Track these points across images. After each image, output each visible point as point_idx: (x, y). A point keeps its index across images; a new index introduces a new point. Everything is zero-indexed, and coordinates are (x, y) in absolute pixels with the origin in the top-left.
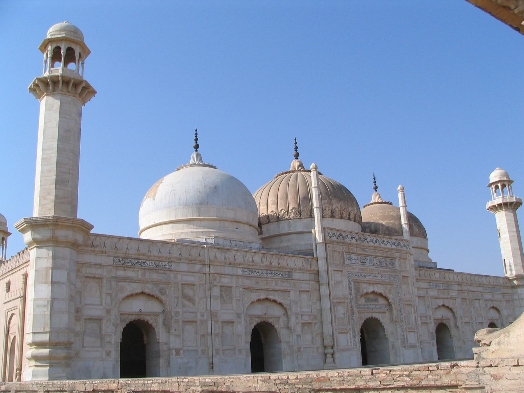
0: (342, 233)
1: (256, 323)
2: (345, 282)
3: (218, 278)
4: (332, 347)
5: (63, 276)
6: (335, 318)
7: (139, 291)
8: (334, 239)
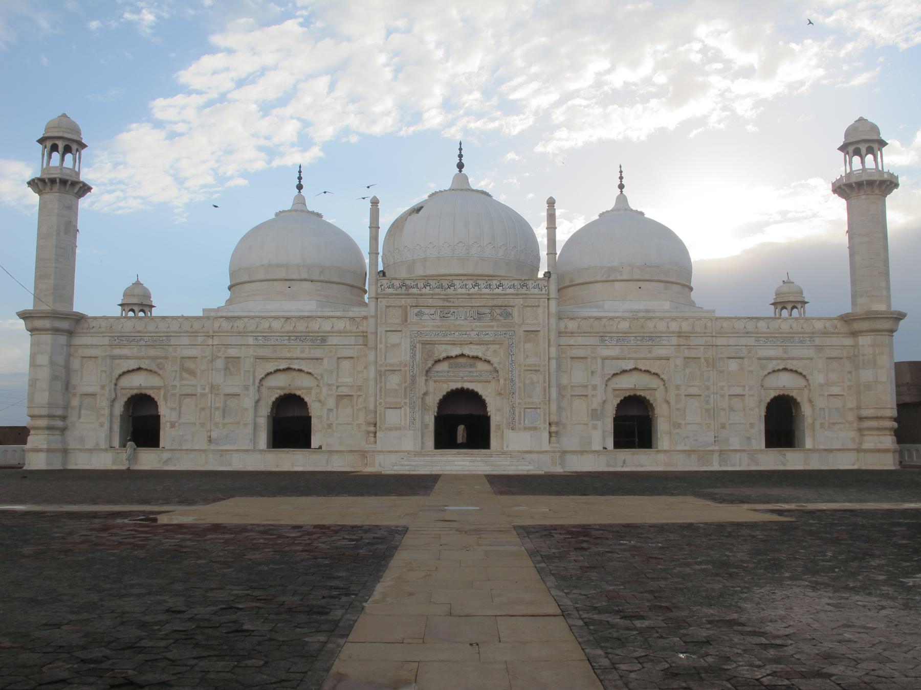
0: (408, 283)
1: (277, 396)
2: (406, 345)
3: (223, 349)
4: (375, 425)
5: (43, 359)
6: (381, 390)
8: (391, 291)
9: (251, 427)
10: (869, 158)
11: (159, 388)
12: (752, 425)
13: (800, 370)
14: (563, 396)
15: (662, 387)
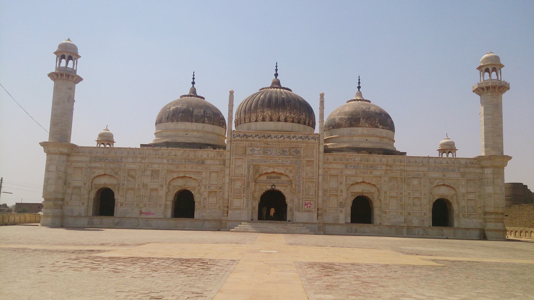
0: (247, 134)
1: (178, 190)
2: (245, 166)
4: (228, 208)
5: (53, 168)
6: (231, 189)
7: (103, 173)
8: (238, 138)
9: (163, 206)
10: (494, 74)
11: (115, 185)
12: (425, 214)
13: (452, 185)
14: (325, 195)
15: (377, 192)
